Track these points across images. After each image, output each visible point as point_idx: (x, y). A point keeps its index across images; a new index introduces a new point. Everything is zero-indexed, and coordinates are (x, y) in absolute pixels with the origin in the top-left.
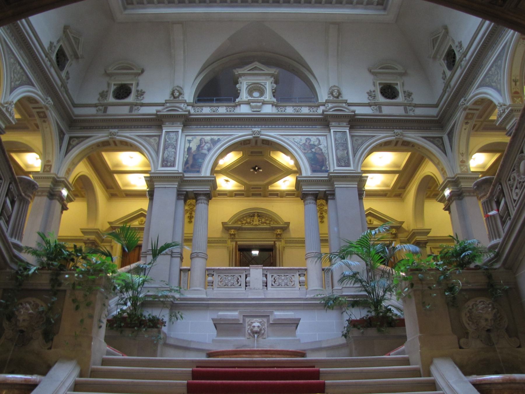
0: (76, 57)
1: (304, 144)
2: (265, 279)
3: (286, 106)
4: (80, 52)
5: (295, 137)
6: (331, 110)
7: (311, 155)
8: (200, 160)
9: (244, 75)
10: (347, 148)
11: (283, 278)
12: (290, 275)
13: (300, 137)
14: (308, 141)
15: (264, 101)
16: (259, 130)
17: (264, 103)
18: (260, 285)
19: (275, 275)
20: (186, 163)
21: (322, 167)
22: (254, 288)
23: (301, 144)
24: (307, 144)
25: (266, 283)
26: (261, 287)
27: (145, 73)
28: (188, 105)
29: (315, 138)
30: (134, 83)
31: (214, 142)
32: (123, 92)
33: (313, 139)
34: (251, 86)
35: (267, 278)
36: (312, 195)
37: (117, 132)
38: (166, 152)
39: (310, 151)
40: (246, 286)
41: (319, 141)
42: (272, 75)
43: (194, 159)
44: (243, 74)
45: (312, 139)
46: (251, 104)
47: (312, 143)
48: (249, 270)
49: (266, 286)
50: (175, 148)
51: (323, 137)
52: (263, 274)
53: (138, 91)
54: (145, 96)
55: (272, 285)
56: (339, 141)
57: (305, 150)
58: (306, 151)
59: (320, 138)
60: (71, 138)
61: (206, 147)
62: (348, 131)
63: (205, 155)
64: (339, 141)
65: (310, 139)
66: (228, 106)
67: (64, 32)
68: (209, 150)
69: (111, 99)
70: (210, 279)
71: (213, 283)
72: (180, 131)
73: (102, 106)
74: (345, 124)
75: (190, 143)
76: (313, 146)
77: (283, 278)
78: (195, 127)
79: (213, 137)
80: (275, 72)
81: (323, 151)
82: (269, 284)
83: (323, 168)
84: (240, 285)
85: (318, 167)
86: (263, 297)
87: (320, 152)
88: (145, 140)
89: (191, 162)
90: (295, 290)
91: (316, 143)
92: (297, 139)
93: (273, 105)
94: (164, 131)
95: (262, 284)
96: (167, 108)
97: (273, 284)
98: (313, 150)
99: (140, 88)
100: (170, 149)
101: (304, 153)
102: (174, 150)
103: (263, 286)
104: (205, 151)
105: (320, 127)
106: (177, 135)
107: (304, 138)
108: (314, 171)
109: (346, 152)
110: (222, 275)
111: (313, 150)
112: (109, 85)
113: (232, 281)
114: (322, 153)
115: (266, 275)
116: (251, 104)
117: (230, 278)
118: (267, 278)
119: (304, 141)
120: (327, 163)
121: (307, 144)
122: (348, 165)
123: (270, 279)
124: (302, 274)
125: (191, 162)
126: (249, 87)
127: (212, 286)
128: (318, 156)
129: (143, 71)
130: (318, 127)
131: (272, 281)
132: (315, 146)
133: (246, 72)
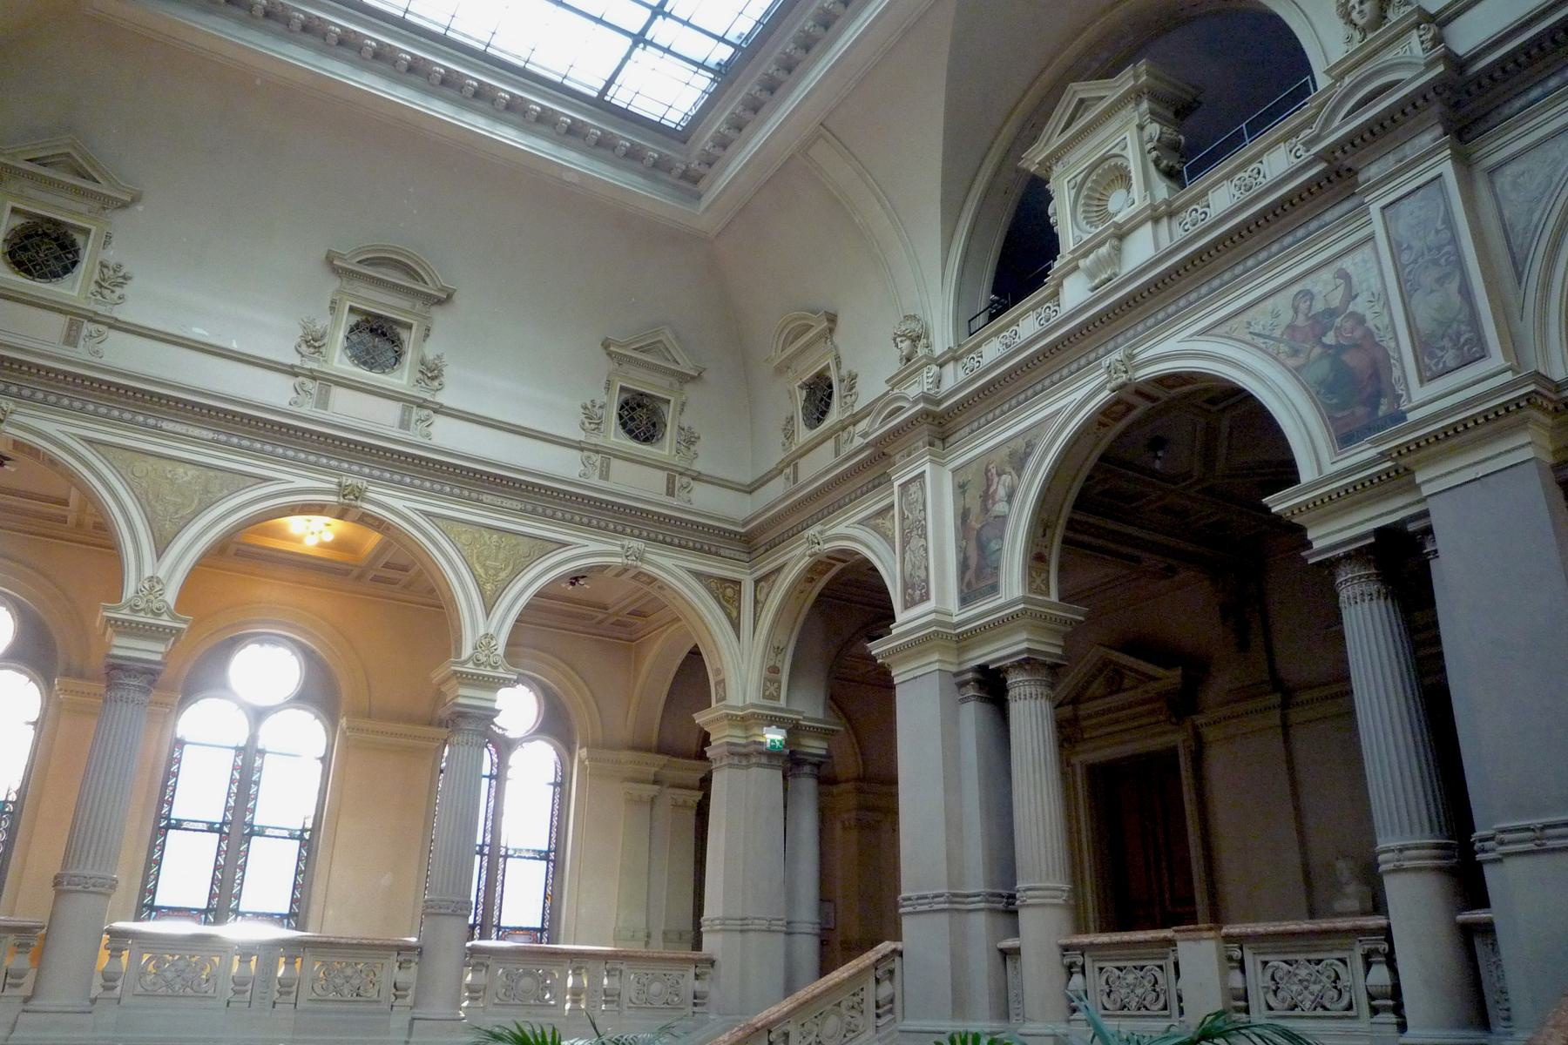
0: (684, 378)
1: (1291, 328)
3: (1204, 193)
4: (686, 366)
5: (1244, 318)
6: (1336, 123)
7: (1323, 369)
8: (994, 546)
9: (1056, 156)
10: (1460, 263)
11: (1303, 973)
12: (1330, 957)
13: (1269, 303)
14: (1303, 306)
15: (1118, 226)
16: (1117, 355)
17: (1121, 234)
19: (1275, 961)
20: (963, 566)
21: (1376, 407)
23: (1277, 333)
24: (1301, 321)
27: (840, 320)
28: (941, 366)
29: (1326, 274)
30: (830, 361)
31: (1018, 461)
32: (819, 395)
33: (1324, 288)
34: (1088, 184)
36: (1348, 556)
37: (821, 533)
38: (907, 557)
39: (1318, 350)
40: (1182, 1012)
41: (1344, 276)
42: (1136, 95)
43: (982, 547)
44: (1048, 158)
45: (1315, 290)
46: (1082, 263)
47: (1319, 306)
50: (924, 536)
51: (1358, 256)
53: (842, 381)
54: (858, 388)
56: (1417, 244)
57: (1295, 353)
58: (1301, 360)
59: (1347, 263)
60: (757, 582)
61: (1002, 492)
62: (1447, 169)
63: (1003, 518)
64: (1417, 244)
65: (1308, 295)
66: (1039, 304)
67: (609, 354)
68: (1010, 497)
69: (804, 435)
72: (927, 467)
73: (788, 465)
74: (1426, 140)
75: (964, 493)
76: (1323, 321)
78: (967, 429)
79: (1012, 445)
80: (1136, 77)
81: (1370, 324)
83: (1383, 409)
84: (1165, 1008)
85: (1360, 411)
87: (1358, 333)
88: (876, 529)
89: (973, 562)
91: (1336, 300)
92: (1260, 318)
93: (1156, 220)
94: (896, 484)
96: (879, 413)
98: (1329, 339)
99: (844, 372)
100: (916, 542)
101: (1296, 372)
102: (922, 542)
104: (1000, 508)
105: (1337, 211)
106: (923, 488)
107: (1283, 301)
108: (1345, 439)
109: (1453, 286)
110: (1109, 965)
111: (1329, 339)
112: (791, 395)
114: (1369, 334)
116: (1082, 263)
117: (1130, 978)
119: (1287, 317)
120: (1396, 373)
121: (1301, 321)
122: (1474, 352)
123: (1257, 979)
125: (973, 562)
126: (1084, 192)
128: (1351, 359)
129: (832, 319)
130: (1328, 217)
132: (1331, 313)
133: (1057, 142)
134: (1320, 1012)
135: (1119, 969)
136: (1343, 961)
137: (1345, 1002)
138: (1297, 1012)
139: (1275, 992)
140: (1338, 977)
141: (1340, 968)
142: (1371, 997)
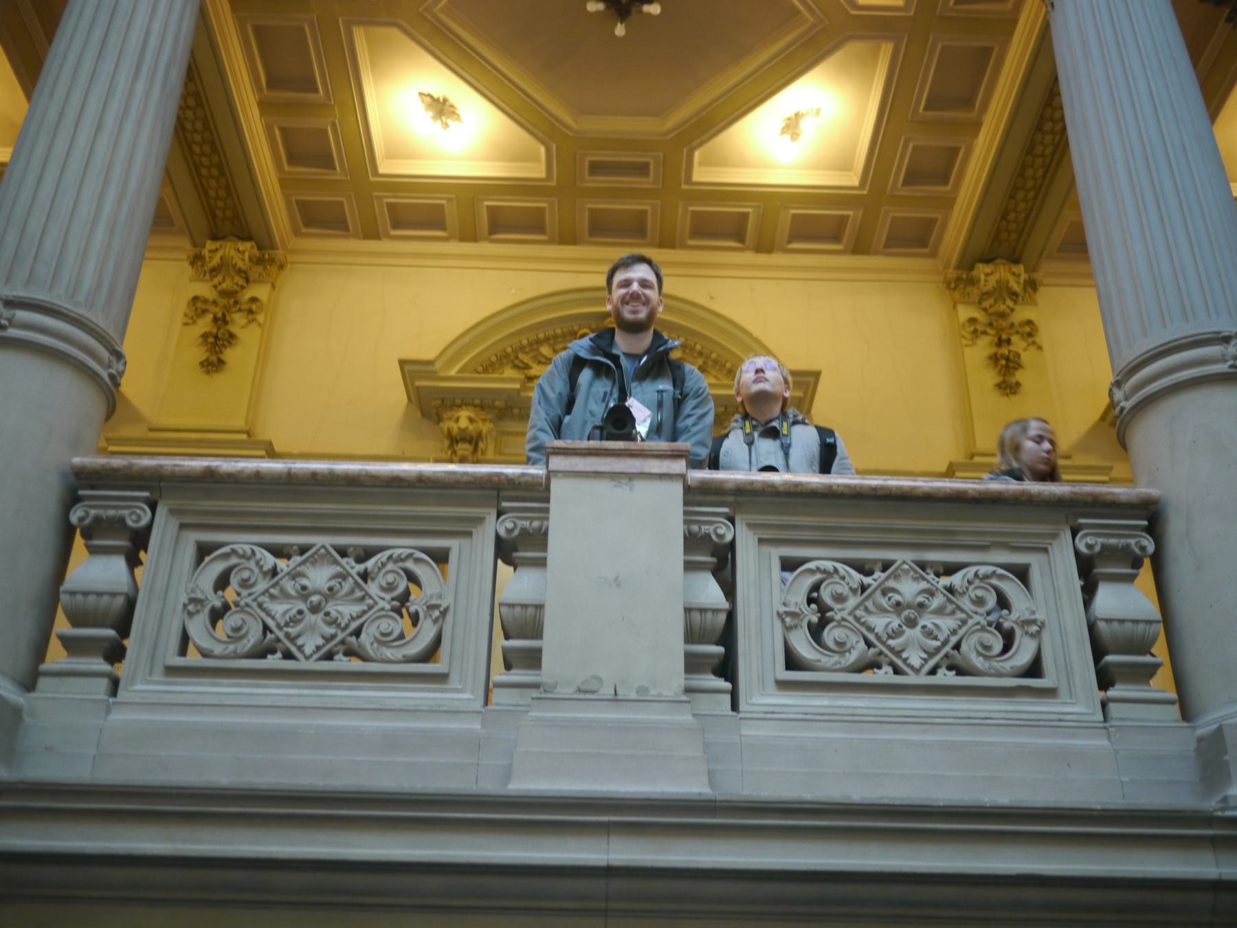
2: (710, 592)
11: (909, 589)
18: (662, 657)
19: (822, 558)
22: (586, 693)
25: (728, 636)
26: (674, 677)
35: (729, 590)
48: (538, 492)
49: (727, 668)
52: (692, 542)
55: (792, 662)
70: (97, 572)
71: (124, 624)
77: (909, 589)
82: (758, 652)
84: (430, 654)
86: (695, 787)
90: (1057, 725)
95: (677, 647)
97: (804, 647)
103: (693, 664)
110: (243, 541)
113: (346, 610)
115: (722, 563)
117: (319, 577)
118: (729, 590)
123: (766, 592)
124: (1109, 554)
127: (115, 654)
131: (788, 619)
134: (946, 677)
135: (278, 551)
136: (1022, 573)
137: (1023, 655)
138: (883, 675)
139: (816, 632)
140: (1003, 602)
141: (1012, 589)
142: (1098, 650)
